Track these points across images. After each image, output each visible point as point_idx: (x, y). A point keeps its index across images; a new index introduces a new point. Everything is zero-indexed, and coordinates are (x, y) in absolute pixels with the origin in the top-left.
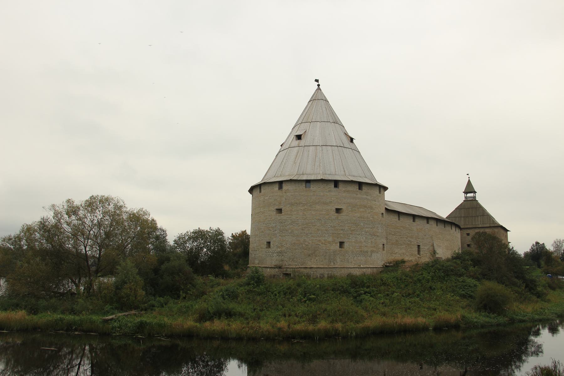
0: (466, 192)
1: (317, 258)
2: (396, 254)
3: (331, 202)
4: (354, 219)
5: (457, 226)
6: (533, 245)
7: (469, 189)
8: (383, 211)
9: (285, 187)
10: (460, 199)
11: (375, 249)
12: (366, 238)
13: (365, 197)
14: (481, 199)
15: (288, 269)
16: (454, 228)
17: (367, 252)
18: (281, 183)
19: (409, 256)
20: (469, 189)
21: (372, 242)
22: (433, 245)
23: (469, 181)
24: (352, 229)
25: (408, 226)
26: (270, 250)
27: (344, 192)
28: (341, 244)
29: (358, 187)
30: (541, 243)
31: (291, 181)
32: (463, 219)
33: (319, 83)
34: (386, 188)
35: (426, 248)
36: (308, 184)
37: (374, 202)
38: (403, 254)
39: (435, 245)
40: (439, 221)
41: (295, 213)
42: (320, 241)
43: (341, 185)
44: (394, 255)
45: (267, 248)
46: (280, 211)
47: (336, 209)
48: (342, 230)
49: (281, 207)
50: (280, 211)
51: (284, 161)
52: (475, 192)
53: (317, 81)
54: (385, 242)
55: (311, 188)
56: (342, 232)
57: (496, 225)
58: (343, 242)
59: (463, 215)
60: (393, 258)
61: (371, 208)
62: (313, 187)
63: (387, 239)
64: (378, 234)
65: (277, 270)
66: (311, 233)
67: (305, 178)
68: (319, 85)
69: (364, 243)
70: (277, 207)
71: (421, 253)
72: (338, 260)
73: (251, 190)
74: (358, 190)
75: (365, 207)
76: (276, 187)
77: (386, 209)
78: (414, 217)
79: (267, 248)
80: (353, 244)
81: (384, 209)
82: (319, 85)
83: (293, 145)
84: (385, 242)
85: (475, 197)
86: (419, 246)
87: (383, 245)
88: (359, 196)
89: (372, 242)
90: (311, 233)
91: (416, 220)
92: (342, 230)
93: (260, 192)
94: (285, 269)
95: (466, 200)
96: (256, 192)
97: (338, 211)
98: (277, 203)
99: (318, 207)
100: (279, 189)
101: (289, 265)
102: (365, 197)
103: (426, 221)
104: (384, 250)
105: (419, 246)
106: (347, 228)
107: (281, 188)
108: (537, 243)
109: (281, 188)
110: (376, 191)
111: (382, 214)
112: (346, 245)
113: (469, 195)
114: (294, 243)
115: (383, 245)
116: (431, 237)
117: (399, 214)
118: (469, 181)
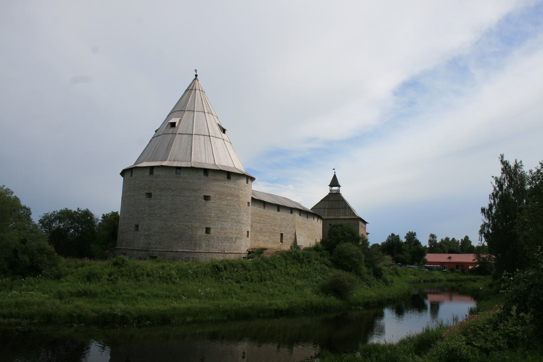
0: (331, 185)
1: (183, 242)
2: (259, 241)
4: (221, 206)
5: (319, 217)
6: (389, 236)
7: (334, 182)
8: (250, 201)
9: (156, 172)
10: (325, 191)
11: (239, 236)
12: (231, 224)
14: (346, 192)
15: (155, 253)
16: (316, 219)
17: (231, 238)
19: (271, 244)
20: (334, 182)
21: (237, 229)
23: (335, 176)
24: (219, 216)
28: (208, 230)
29: (226, 176)
30: (396, 235)
32: (326, 210)
33: (197, 74)
34: (253, 179)
35: (289, 236)
36: (178, 171)
38: (267, 241)
39: (297, 234)
40: (303, 212)
42: (187, 226)
43: (210, 174)
44: (258, 242)
45: (135, 230)
46: (149, 195)
49: (151, 191)
50: (149, 195)
51: (158, 147)
52: (339, 186)
53: (196, 71)
54: (249, 229)
55: (182, 175)
56: (208, 218)
57: (356, 217)
58: (210, 228)
59: (327, 207)
60: (257, 244)
62: (184, 174)
63: (252, 226)
65: (144, 253)
66: (179, 218)
67: (175, 164)
68: (196, 76)
69: (229, 230)
70: (146, 192)
71: (284, 241)
72: (204, 245)
73: (123, 173)
74: (226, 179)
75: (232, 195)
76: (147, 173)
77: (252, 198)
78: (279, 207)
79: (135, 230)
80: (219, 230)
81: (251, 198)
82: (196, 76)
83: (166, 132)
84: (249, 229)
85: (338, 191)
86: (282, 235)
87: (248, 232)
89: (237, 229)
90: (179, 218)
91: (281, 210)
93: (132, 175)
95: (331, 194)
96: (128, 175)
97: (207, 198)
100: (150, 174)
101: (156, 248)
104: (248, 237)
105: (282, 235)
106: (213, 214)
108: (393, 235)
110: (244, 181)
111: (249, 203)
112: (212, 231)
113: (334, 188)
115: (248, 232)
116: (294, 227)
117: (264, 204)
118: (335, 176)
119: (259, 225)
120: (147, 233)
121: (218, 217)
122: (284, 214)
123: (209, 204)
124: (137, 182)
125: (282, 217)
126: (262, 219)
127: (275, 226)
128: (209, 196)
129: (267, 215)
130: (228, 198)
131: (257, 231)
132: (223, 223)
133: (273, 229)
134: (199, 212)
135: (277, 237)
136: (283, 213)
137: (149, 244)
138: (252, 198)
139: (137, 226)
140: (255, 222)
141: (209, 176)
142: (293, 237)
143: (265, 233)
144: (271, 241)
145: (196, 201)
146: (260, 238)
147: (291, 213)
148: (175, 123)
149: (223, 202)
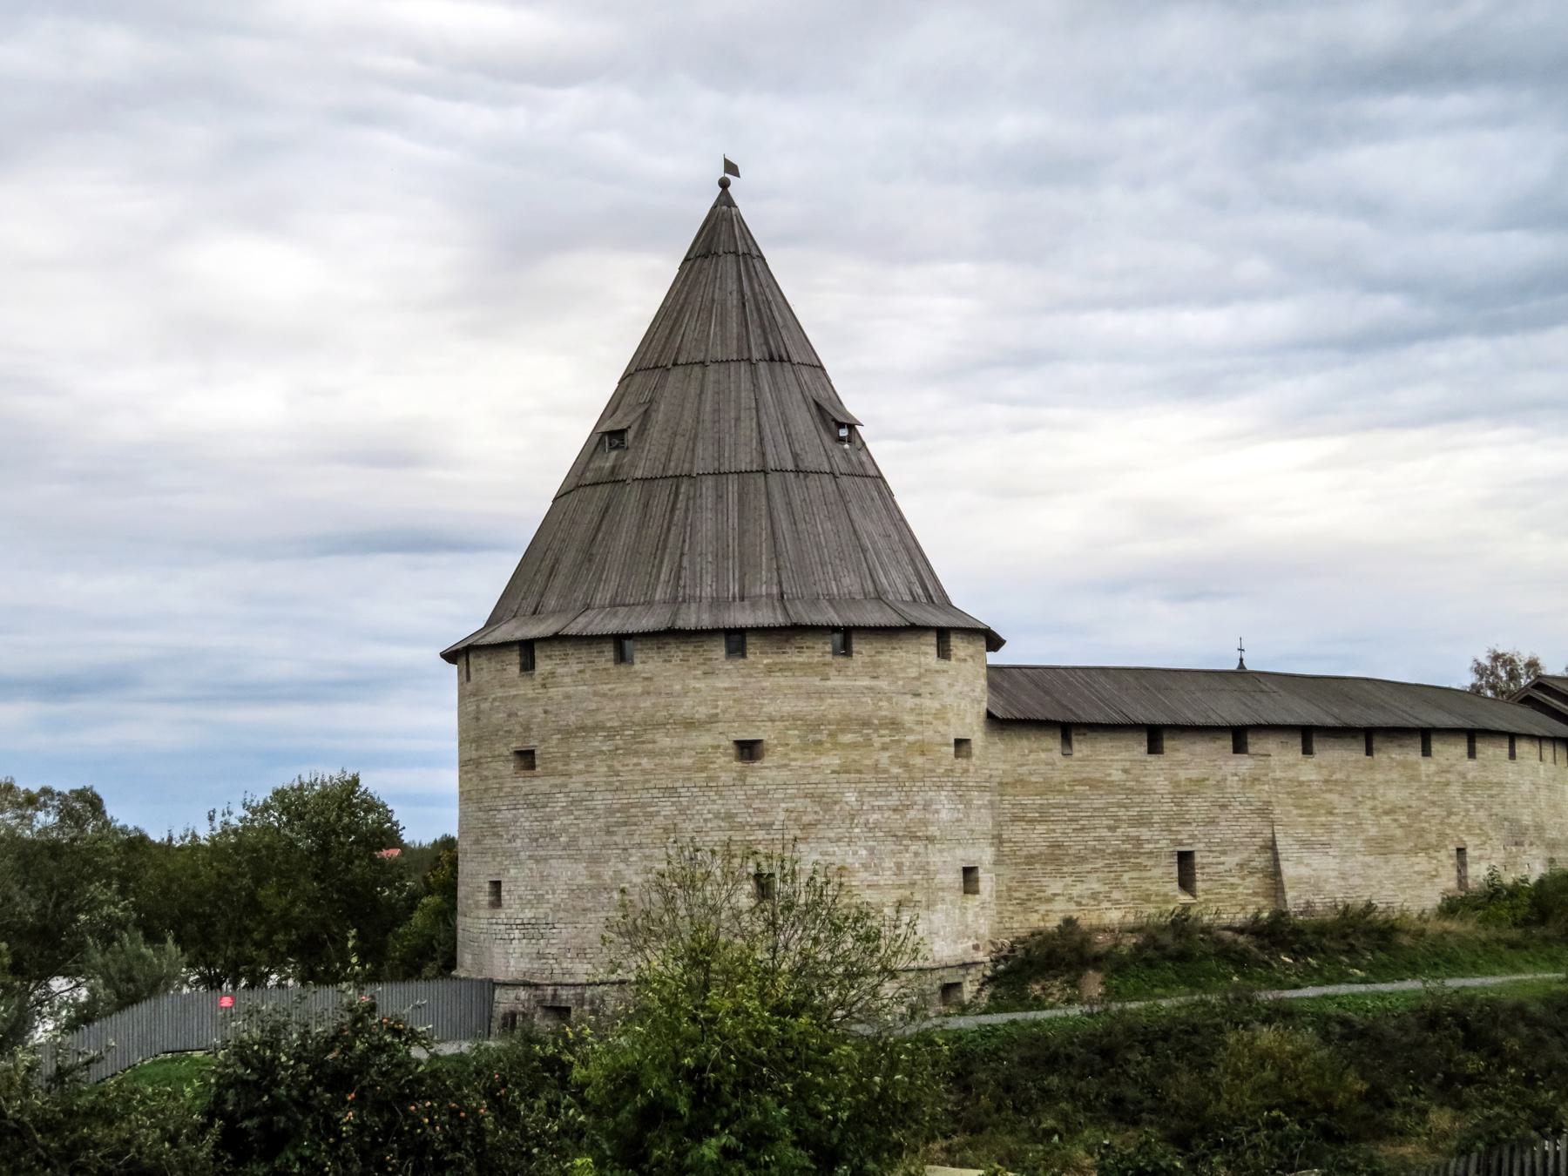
2: (1049, 900)
3: (713, 719)
4: (815, 778)
12: (871, 851)
13: (866, 682)
18: (527, 649)
19: (1111, 905)
22: (1271, 846)
24: (806, 819)
25: (1116, 775)
26: (502, 915)
27: (769, 670)
31: (557, 639)
35: (1231, 860)
37: (910, 702)
38: (1094, 896)
39: (1281, 843)
41: (581, 766)
43: (753, 644)
44: (1043, 908)
47: (738, 743)
48: (761, 826)
49: (533, 743)
54: (983, 855)
55: (638, 666)
56: (760, 835)
61: (894, 725)
63: (998, 840)
64: (933, 830)
65: (523, 994)
66: (640, 846)
69: (863, 875)
70: (516, 745)
71: (1199, 885)
75: (866, 723)
84: (983, 855)
88: (836, 682)
89: (899, 866)
90: (640, 846)
91: (1168, 744)
92: (761, 826)
94: (550, 990)
97: (748, 750)
98: (518, 729)
99: (664, 741)
102: (866, 682)
103: (1227, 743)
107: (528, 666)
109: (528, 666)
111: (959, 743)
114: (580, 887)
119: (1041, 828)
120: (528, 914)
121: (804, 827)
122: (1192, 761)
123: (765, 772)
124: (485, 706)
125: (1182, 775)
126: (1060, 799)
127: (1142, 821)
128: (759, 741)
129: (1082, 782)
130: (848, 738)
131: (1030, 860)
132: (832, 848)
133: (1128, 839)
134: (717, 816)
135: (1157, 872)
136: (1182, 756)
137: (540, 956)
138: (990, 715)
139: (496, 885)
140: (1015, 819)
141: (751, 657)
142: (1260, 861)
143: (1083, 860)
144: (1116, 895)
145: (702, 770)
146: (1055, 886)
147: (1239, 748)
148: (622, 432)
149: (824, 760)
